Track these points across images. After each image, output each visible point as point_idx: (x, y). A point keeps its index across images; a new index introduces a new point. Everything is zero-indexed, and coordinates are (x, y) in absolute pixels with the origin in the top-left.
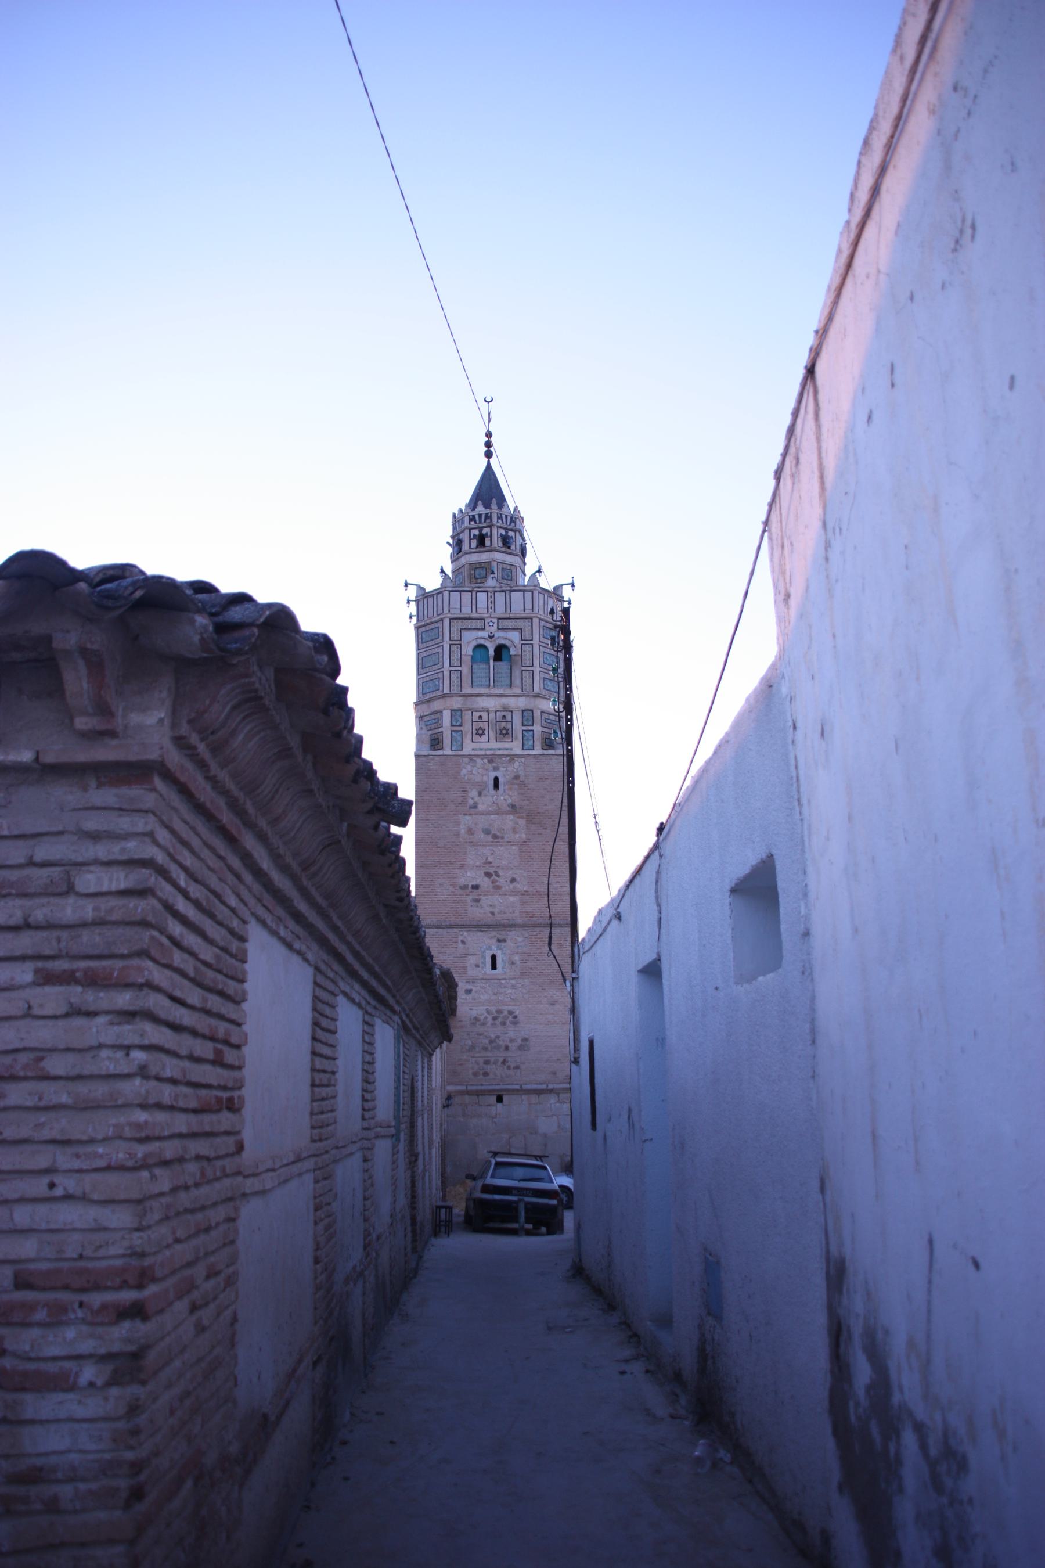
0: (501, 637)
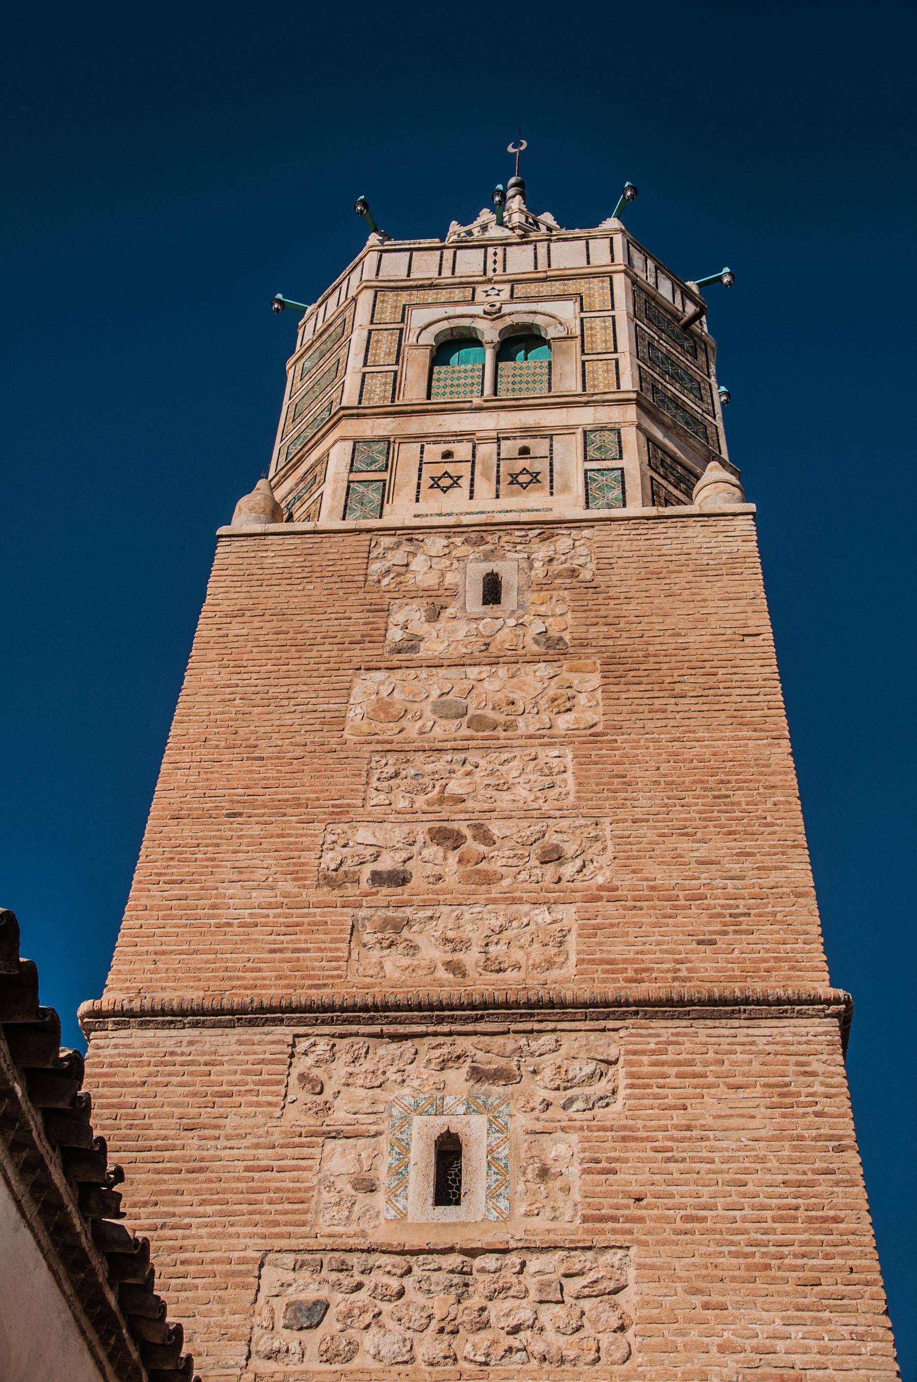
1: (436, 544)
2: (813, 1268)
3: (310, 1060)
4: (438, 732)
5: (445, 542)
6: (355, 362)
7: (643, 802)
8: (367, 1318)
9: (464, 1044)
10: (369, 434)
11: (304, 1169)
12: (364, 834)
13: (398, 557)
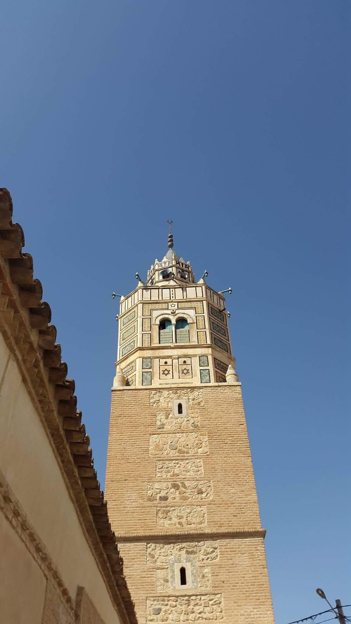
0: (181, 313)
1: (165, 393)
2: (258, 596)
3: (151, 549)
4: (171, 455)
5: (168, 393)
6: (140, 329)
7: (219, 476)
8: (169, 612)
9: (184, 545)
10: (146, 356)
11: (153, 577)
12: (156, 485)
13: (156, 398)
